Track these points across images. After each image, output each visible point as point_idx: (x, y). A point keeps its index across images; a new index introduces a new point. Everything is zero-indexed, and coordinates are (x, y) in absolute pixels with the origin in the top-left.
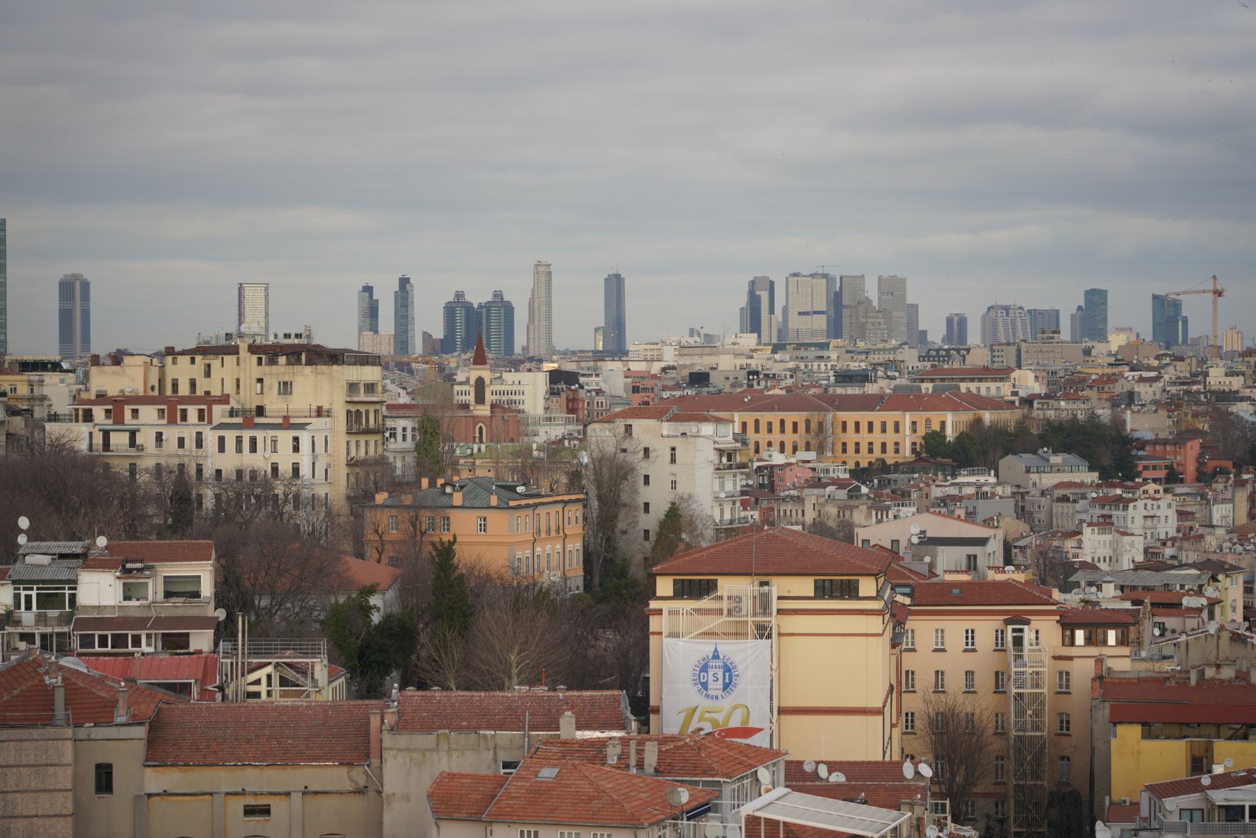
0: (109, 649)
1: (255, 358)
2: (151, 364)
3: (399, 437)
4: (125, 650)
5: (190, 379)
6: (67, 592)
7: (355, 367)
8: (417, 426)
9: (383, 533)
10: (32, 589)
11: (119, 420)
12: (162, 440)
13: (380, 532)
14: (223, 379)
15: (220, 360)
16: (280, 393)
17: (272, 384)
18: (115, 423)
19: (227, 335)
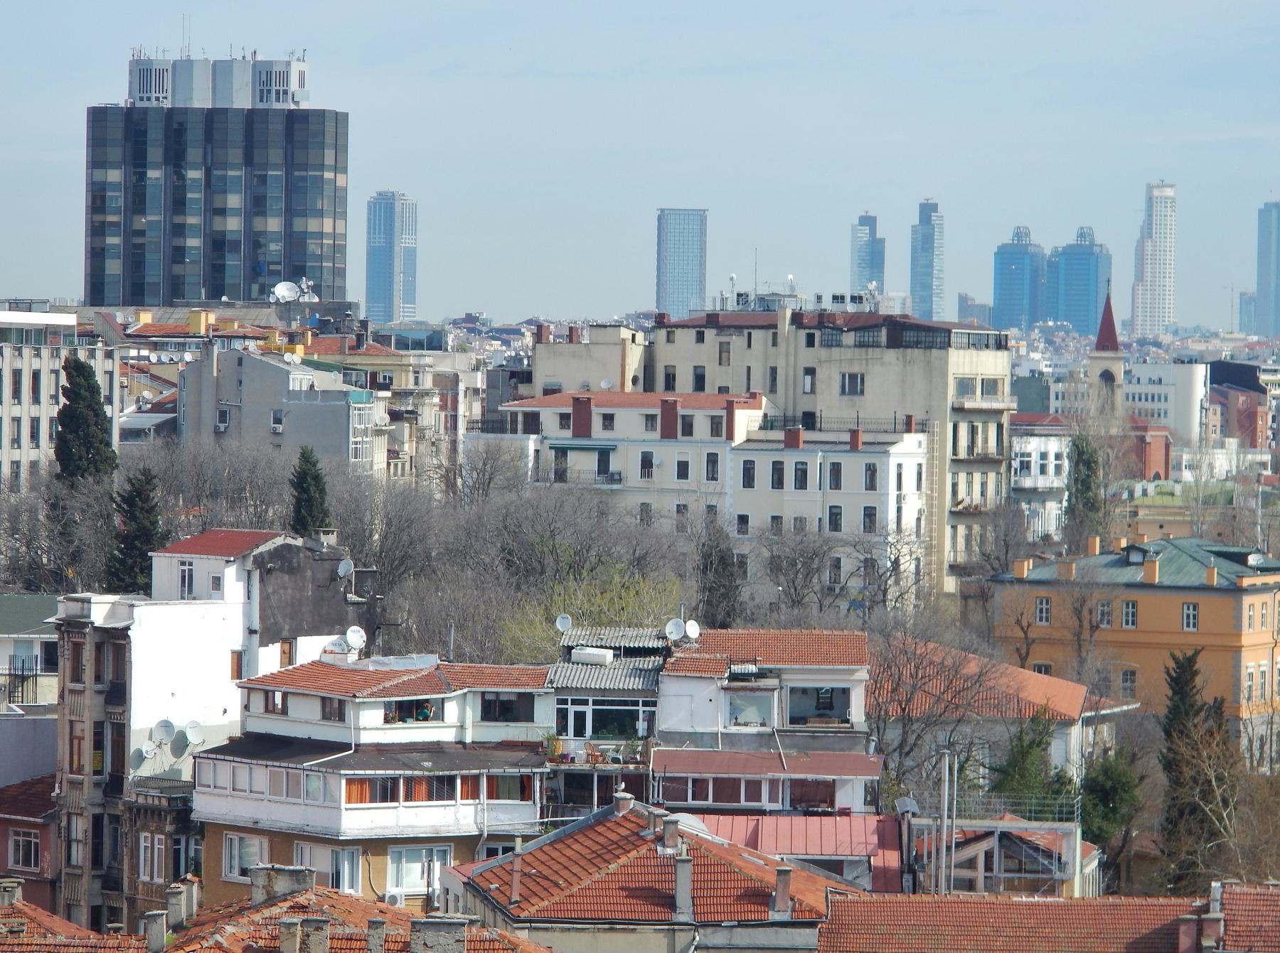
0: (710, 802)
1: (802, 334)
2: (633, 341)
3: (1035, 468)
4: (735, 805)
5: (695, 368)
6: (641, 708)
7: (968, 352)
8: (1066, 451)
9: (1029, 625)
10: (585, 703)
11: (583, 429)
12: (651, 466)
13: (1025, 624)
14: (749, 368)
15: (746, 335)
16: (843, 392)
17: (830, 379)
18: (575, 435)
19: (739, 295)
